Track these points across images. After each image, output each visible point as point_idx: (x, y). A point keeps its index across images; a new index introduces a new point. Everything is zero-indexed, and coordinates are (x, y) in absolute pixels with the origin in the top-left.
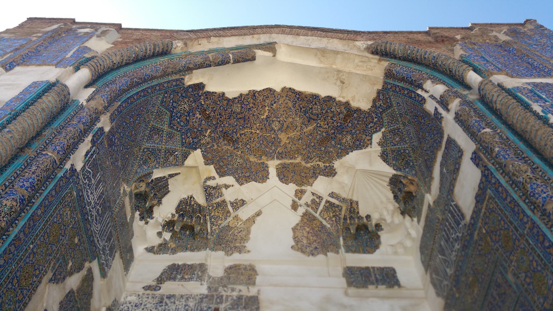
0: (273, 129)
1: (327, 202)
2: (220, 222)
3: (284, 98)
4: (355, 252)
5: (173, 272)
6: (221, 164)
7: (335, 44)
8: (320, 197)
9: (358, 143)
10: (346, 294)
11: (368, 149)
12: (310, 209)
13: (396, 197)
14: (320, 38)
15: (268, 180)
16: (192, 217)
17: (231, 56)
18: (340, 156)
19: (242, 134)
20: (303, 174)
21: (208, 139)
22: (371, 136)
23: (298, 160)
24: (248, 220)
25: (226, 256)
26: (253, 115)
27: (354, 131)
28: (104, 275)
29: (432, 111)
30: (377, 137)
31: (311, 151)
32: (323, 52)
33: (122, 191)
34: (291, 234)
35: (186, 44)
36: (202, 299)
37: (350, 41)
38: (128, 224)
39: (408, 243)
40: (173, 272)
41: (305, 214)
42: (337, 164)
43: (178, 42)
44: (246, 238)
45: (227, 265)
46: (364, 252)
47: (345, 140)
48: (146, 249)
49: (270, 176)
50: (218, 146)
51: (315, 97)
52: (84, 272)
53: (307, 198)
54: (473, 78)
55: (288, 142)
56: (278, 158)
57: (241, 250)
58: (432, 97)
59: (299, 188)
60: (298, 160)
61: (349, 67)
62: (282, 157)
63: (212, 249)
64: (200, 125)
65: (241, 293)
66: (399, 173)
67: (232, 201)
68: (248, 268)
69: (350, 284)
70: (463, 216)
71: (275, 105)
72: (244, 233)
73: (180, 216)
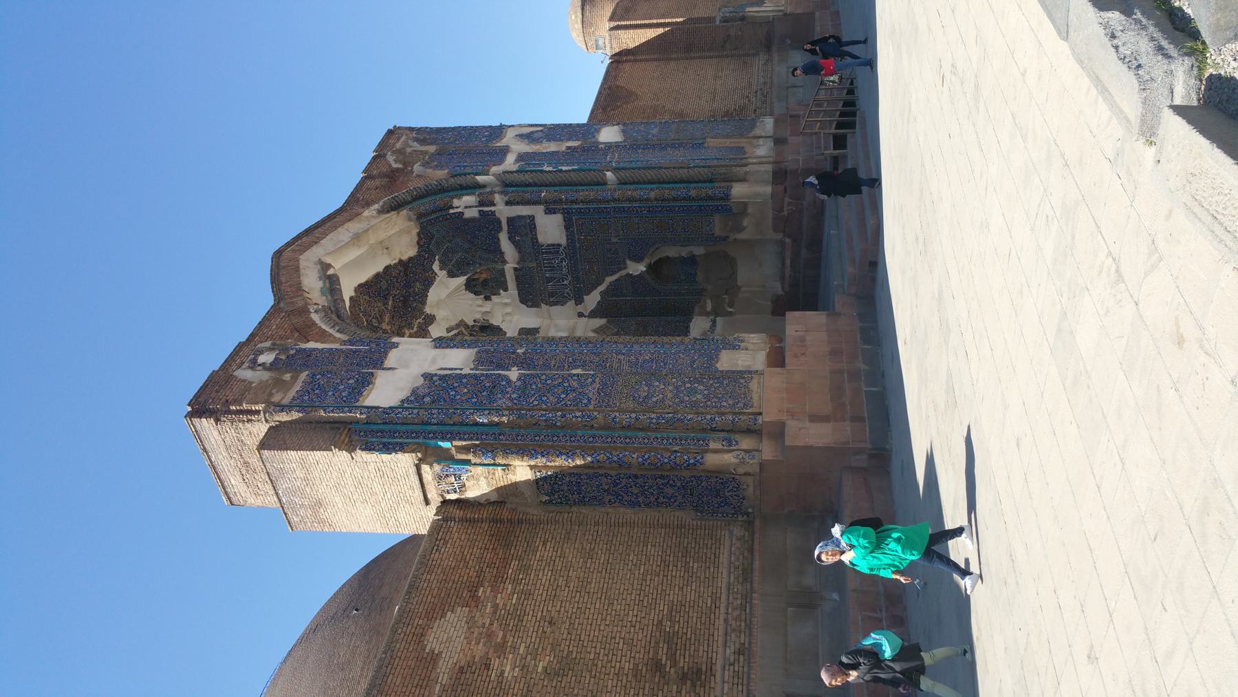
7: (354, 227)
11: (438, 279)
13: (476, 293)
18: (424, 303)
29: (477, 215)
30: (436, 267)
32: (357, 238)
39: (508, 310)
42: (428, 310)
51: (377, 276)
54: (480, 178)
61: (382, 235)
70: (559, 245)
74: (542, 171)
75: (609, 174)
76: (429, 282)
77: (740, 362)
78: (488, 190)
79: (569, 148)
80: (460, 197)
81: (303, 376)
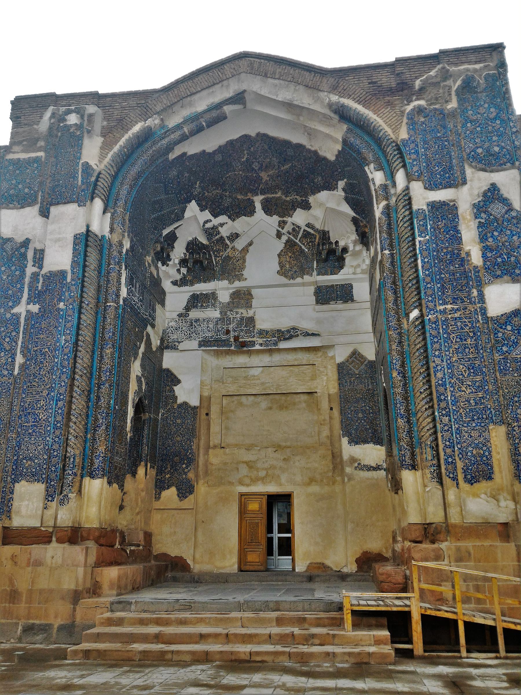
0: (253, 169)
1: (304, 231)
2: (221, 254)
3: (260, 142)
4: (323, 275)
5: (195, 301)
6: (214, 206)
8: (298, 227)
9: (327, 184)
10: (314, 310)
11: (335, 192)
12: (291, 236)
13: (357, 230)
14: (287, 83)
15: (255, 214)
16: (199, 254)
17: (204, 124)
18: (314, 193)
19: (227, 177)
20: (283, 207)
21: (199, 190)
22: (337, 182)
23: (279, 195)
24: (243, 249)
25: (230, 285)
26: (234, 160)
27: (323, 174)
28: (153, 326)
30: (341, 184)
31: (289, 186)
33: (147, 265)
34: (277, 259)
35: (162, 120)
36: (217, 321)
37: (315, 91)
38: (156, 279)
40: (195, 301)
41: (288, 241)
42: (311, 199)
43: (156, 119)
44: (242, 268)
45: (231, 291)
46: (331, 274)
47: (316, 180)
48: (172, 282)
49: (257, 210)
50: (208, 192)
51: (287, 143)
52: (145, 338)
53: (288, 227)
54: (400, 177)
55: (268, 179)
56: (261, 194)
57: (240, 278)
58: (373, 180)
59: (282, 219)
60: (279, 195)
62: (265, 192)
63: (219, 280)
64: (189, 180)
65: (243, 315)
66: (357, 216)
67: (228, 235)
68: (247, 293)
69: (318, 302)
71: (252, 148)
72: (241, 261)
73: (190, 254)
74: (414, 239)
75: (415, 314)
76: (330, 187)
77: (26, 503)
78: (392, 191)
79: (468, 254)
80: (380, 168)
81: (41, 154)
